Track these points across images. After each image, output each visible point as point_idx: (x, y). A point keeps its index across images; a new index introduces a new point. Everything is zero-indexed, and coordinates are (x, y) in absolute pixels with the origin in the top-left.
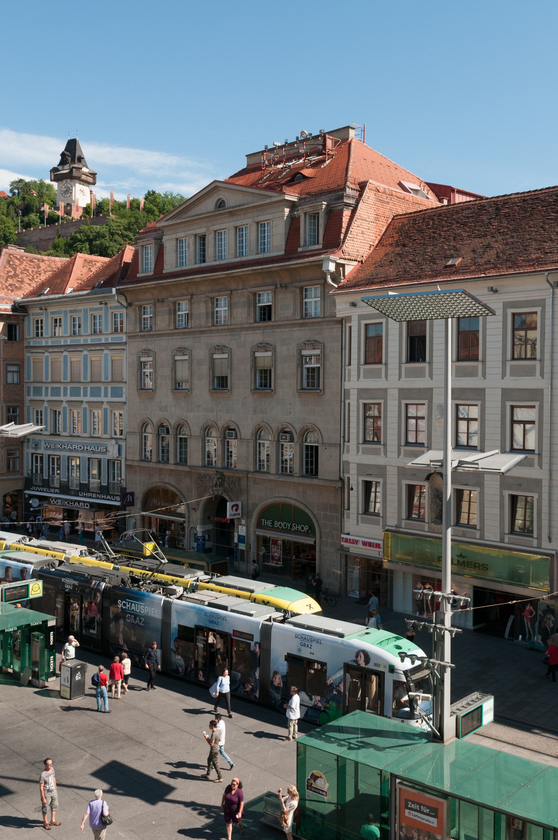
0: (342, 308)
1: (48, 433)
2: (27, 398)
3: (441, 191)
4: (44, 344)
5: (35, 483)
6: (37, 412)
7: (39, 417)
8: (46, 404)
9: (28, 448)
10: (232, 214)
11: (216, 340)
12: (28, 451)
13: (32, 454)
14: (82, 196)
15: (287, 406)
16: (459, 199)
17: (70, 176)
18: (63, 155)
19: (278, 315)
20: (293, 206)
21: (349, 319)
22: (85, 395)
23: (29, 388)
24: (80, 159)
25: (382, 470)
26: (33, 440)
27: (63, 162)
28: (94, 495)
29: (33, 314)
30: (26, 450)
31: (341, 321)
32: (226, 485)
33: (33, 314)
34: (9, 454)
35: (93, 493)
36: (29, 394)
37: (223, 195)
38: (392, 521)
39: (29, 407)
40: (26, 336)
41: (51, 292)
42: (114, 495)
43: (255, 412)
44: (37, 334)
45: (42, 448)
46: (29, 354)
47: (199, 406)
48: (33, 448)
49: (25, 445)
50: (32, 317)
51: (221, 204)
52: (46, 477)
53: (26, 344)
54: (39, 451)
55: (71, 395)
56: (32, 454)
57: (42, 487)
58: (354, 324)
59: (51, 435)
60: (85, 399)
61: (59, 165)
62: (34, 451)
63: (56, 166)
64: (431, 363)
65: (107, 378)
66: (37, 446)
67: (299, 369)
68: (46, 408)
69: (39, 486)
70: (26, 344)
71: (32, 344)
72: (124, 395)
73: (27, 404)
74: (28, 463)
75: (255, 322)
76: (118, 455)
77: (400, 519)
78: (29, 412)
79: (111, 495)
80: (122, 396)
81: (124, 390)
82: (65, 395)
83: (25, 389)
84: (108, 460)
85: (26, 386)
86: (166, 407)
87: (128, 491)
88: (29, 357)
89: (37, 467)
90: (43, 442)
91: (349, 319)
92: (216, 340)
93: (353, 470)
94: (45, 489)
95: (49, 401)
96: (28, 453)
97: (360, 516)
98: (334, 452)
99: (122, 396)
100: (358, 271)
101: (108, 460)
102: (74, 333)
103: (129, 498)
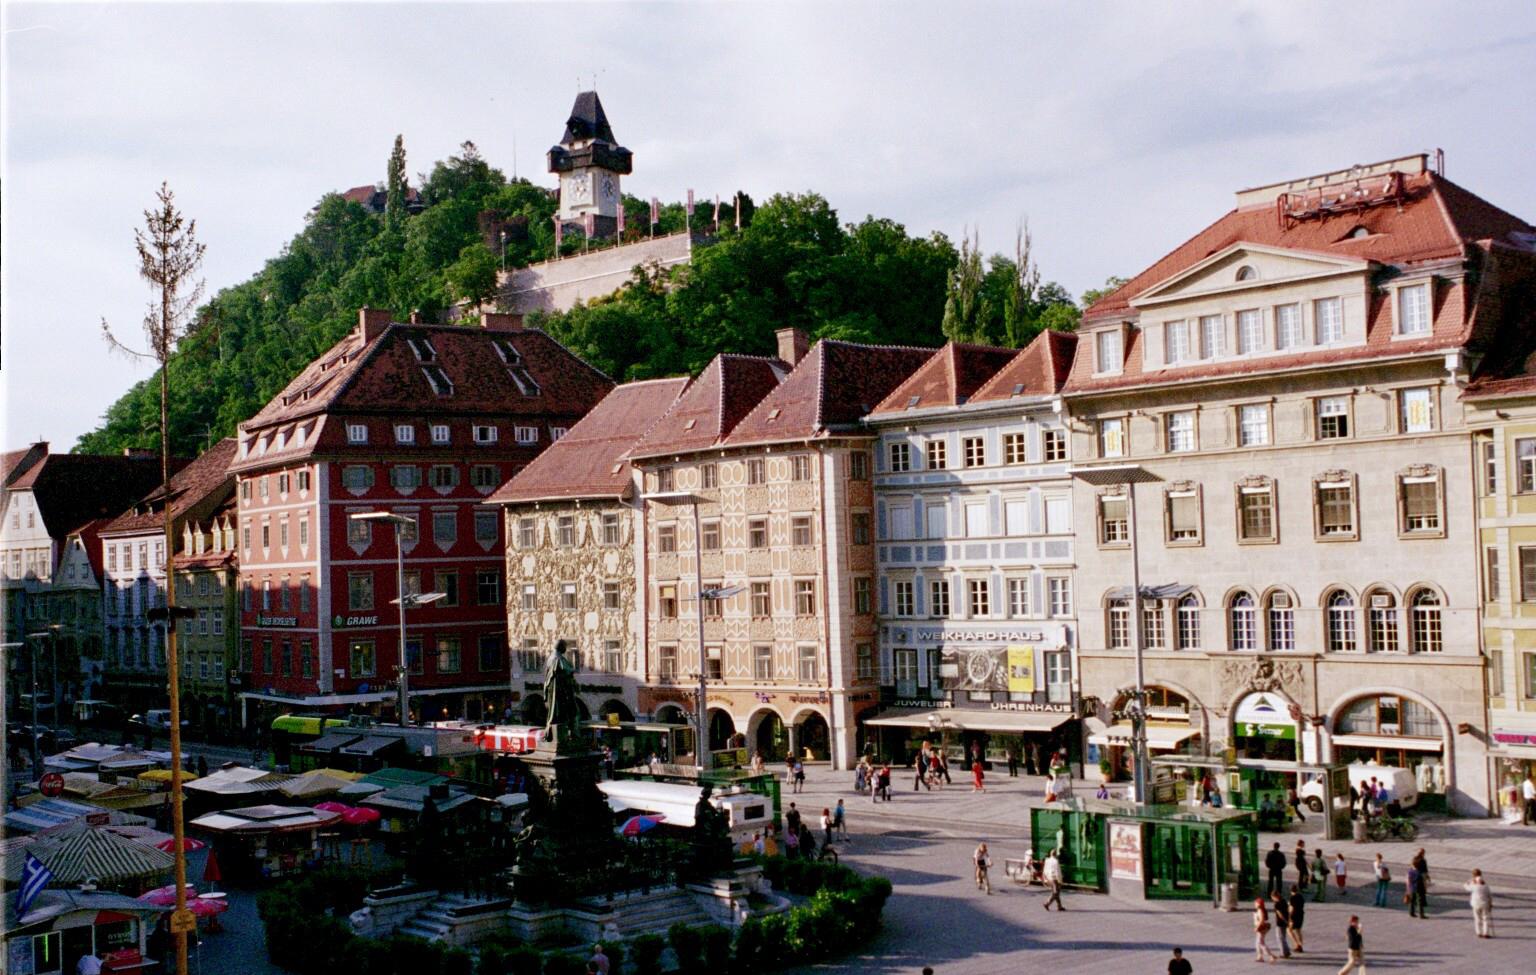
1: (926, 617)
2: (881, 566)
4: (911, 481)
5: (900, 693)
6: (900, 586)
7: (905, 593)
8: (919, 573)
9: (886, 641)
13: (895, 651)
15: (1379, 557)
19: (1359, 428)
22: (996, 554)
23: (883, 550)
26: (895, 629)
28: (1021, 707)
29: (888, 437)
30: (882, 646)
32: (1276, 675)
33: (888, 437)
34: (859, 652)
35: (1018, 703)
36: (883, 558)
39: (884, 579)
40: (875, 470)
42: (1058, 705)
43: (1323, 567)
44: (896, 468)
45: (915, 640)
46: (882, 499)
47: (1217, 564)
48: (896, 640)
49: (881, 638)
50: (885, 443)
52: (923, 684)
53: (875, 483)
54: (907, 646)
55: (968, 557)
56: (895, 651)
57: (917, 699)
59: (931, 619)
60: (1035, 562)
61: (563, 142)
62: (898, 646)
63: (557, 144)
65: (1037, 530)
66: (904, 639)
67: (1401, 504)
68: (920, 579)
69: (911, 699)
70: (875, 483)
71: (887, 482)
72: (1071, 554)
73: (882, 573)
74: (886, 664)
75: (1317, 439)
76: (1064, 643)
78: (885, 588)
79: (1052, 705)
80: (1067, 555)
81: (1071, 546)
83: (878, 552)
84: (1046, 653)
85: (878, 547)
87: (1085, 695)
88: (881, 504)
89: (903, 671)
90: (915, 632)
93: (1508, 637)
94: (923, 703)
95: (924, 568)
96: (886, 651)
97: (1522, 704)
99: (1067, 555)
101: (1046, 653)
102: (933, 465)
103: (1089, 705)
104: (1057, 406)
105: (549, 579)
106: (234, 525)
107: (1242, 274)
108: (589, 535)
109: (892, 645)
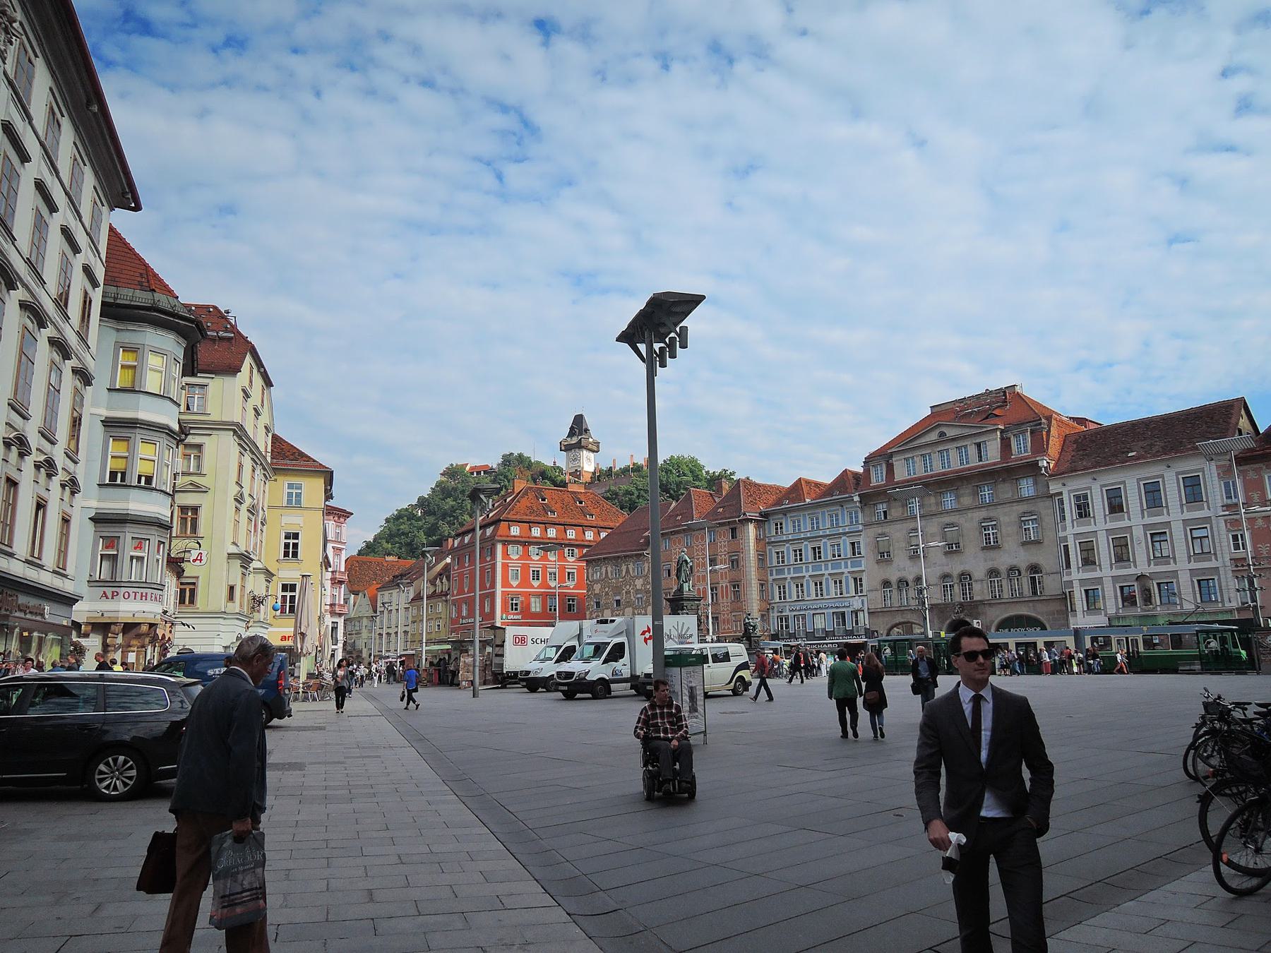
0: (1054, 488)
2: (770, 578)
3: (1081, 421)
10: (954, 440)
11: (947, 519)
12: (774, 615)
14: (588, 463)
16: (1092, 426)
17: (579, 446)
18: (572, 428)
20: (1002, 432)
21: (1061, 494)
24: (587, 430)
25: (1099, 580)
27: (572, 434)
31: (1051, 496)
37: (944, 429)
38: (1112, 611)
41: (792, 501)
51: (942, 434)
58: (1065, 497)
64: (1128, 512)
77: (1118, 609)
82: (807, 571)
86: (901, 567)
91: (1061, 494)
92: (947, 519)
93: (1076, 584)
98: (1057, 577)
100: (1056, 465)
104: (856, 499)
105: (607, 594)
106: (448, 579)
107: (942, 434)
108: (628, 571)
109: (776, 614)
